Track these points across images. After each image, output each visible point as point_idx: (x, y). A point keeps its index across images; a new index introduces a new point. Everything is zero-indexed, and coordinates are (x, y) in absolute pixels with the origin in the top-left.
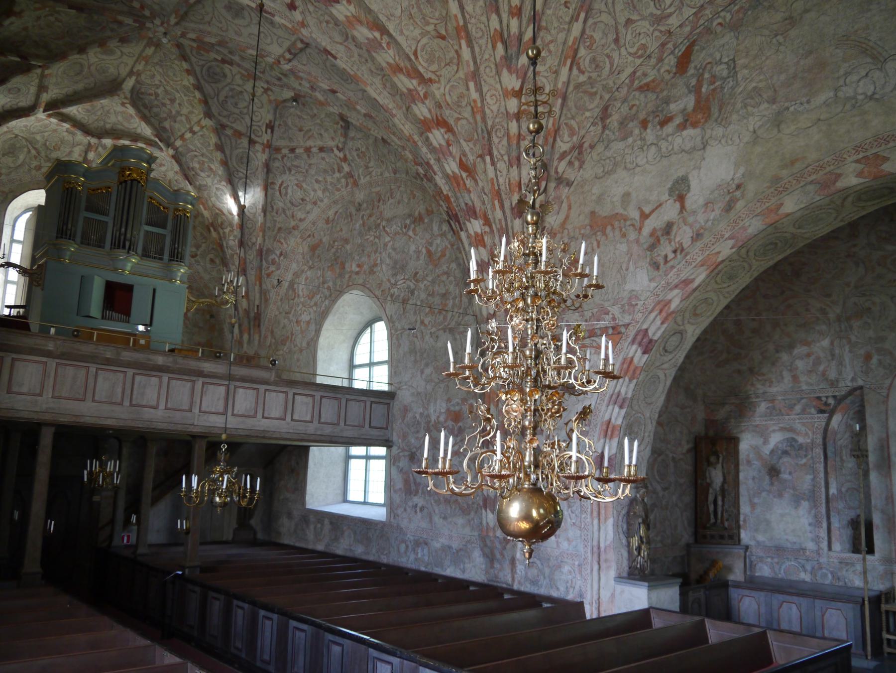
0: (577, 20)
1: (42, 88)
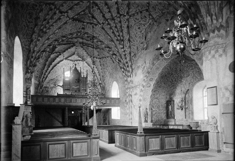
1: (64, 56)
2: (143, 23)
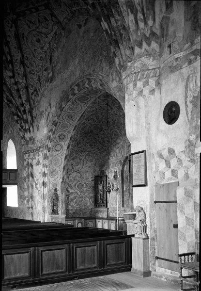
2: (44, 30)
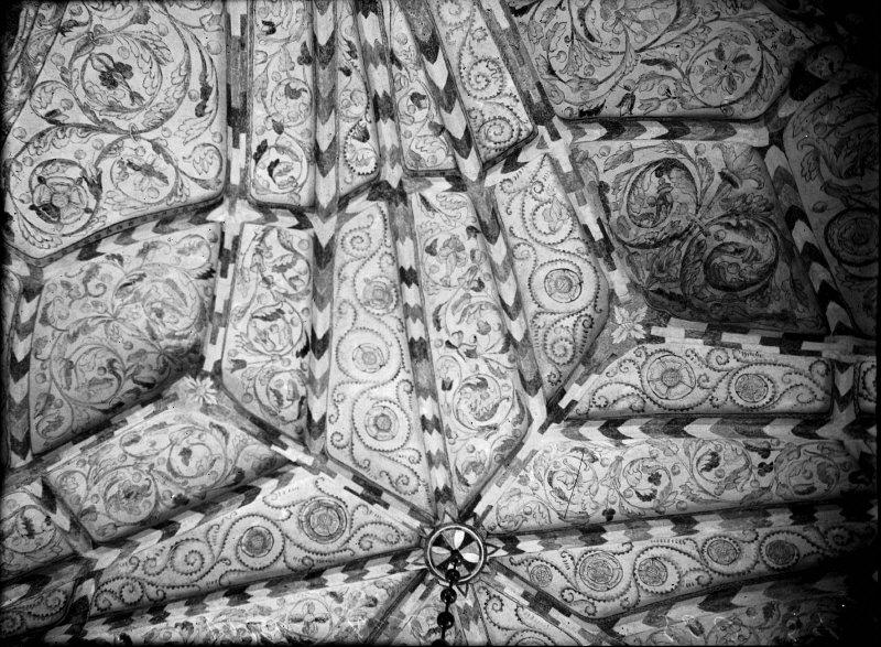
0: (243, 19)
